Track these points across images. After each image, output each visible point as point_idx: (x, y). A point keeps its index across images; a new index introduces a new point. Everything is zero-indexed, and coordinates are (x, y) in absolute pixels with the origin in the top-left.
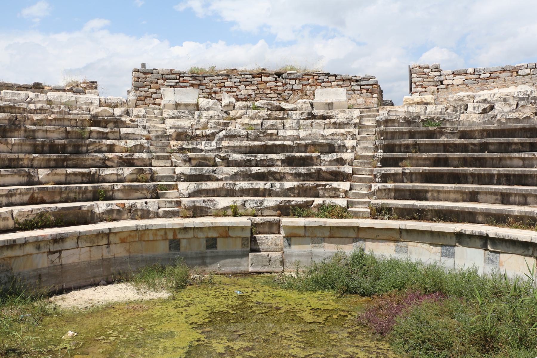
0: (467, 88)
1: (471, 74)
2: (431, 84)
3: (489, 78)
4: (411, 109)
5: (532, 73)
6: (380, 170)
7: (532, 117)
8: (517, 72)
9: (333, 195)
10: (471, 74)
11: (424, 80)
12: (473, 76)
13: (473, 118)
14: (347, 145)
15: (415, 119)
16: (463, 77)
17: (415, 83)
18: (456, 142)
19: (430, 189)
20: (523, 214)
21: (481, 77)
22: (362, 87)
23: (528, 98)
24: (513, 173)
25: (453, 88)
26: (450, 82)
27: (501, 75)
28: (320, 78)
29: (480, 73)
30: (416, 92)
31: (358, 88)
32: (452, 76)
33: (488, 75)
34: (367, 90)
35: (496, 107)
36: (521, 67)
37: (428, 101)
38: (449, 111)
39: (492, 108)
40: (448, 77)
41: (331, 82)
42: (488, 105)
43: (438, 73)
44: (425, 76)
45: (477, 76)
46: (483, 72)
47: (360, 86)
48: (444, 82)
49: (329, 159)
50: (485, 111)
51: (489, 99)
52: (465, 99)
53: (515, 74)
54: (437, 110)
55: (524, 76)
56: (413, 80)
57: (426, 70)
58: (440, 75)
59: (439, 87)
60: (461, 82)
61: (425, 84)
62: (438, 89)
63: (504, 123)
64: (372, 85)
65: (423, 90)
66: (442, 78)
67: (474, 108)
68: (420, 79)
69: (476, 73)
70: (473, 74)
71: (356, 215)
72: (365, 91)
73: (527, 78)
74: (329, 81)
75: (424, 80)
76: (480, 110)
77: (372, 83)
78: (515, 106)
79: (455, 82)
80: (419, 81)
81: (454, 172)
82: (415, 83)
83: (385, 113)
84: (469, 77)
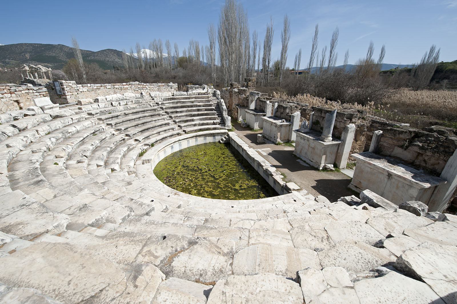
3: (97, 89)
12: (91, 88)
26: (82, 90)
28: (12, 88)
31: (38, 94)
34: (43, 95)
41: (21, 91)
43: (76, 86)
45: (92, 88)
48: (79, 90)
59: (78, 92)
60: (86, 90)
61: (71, 91)
65: (71, 94)
66: (78, 88)
68: (69, 89)
73: (110, 90)
74: (19, 91)
79: (84, 90)
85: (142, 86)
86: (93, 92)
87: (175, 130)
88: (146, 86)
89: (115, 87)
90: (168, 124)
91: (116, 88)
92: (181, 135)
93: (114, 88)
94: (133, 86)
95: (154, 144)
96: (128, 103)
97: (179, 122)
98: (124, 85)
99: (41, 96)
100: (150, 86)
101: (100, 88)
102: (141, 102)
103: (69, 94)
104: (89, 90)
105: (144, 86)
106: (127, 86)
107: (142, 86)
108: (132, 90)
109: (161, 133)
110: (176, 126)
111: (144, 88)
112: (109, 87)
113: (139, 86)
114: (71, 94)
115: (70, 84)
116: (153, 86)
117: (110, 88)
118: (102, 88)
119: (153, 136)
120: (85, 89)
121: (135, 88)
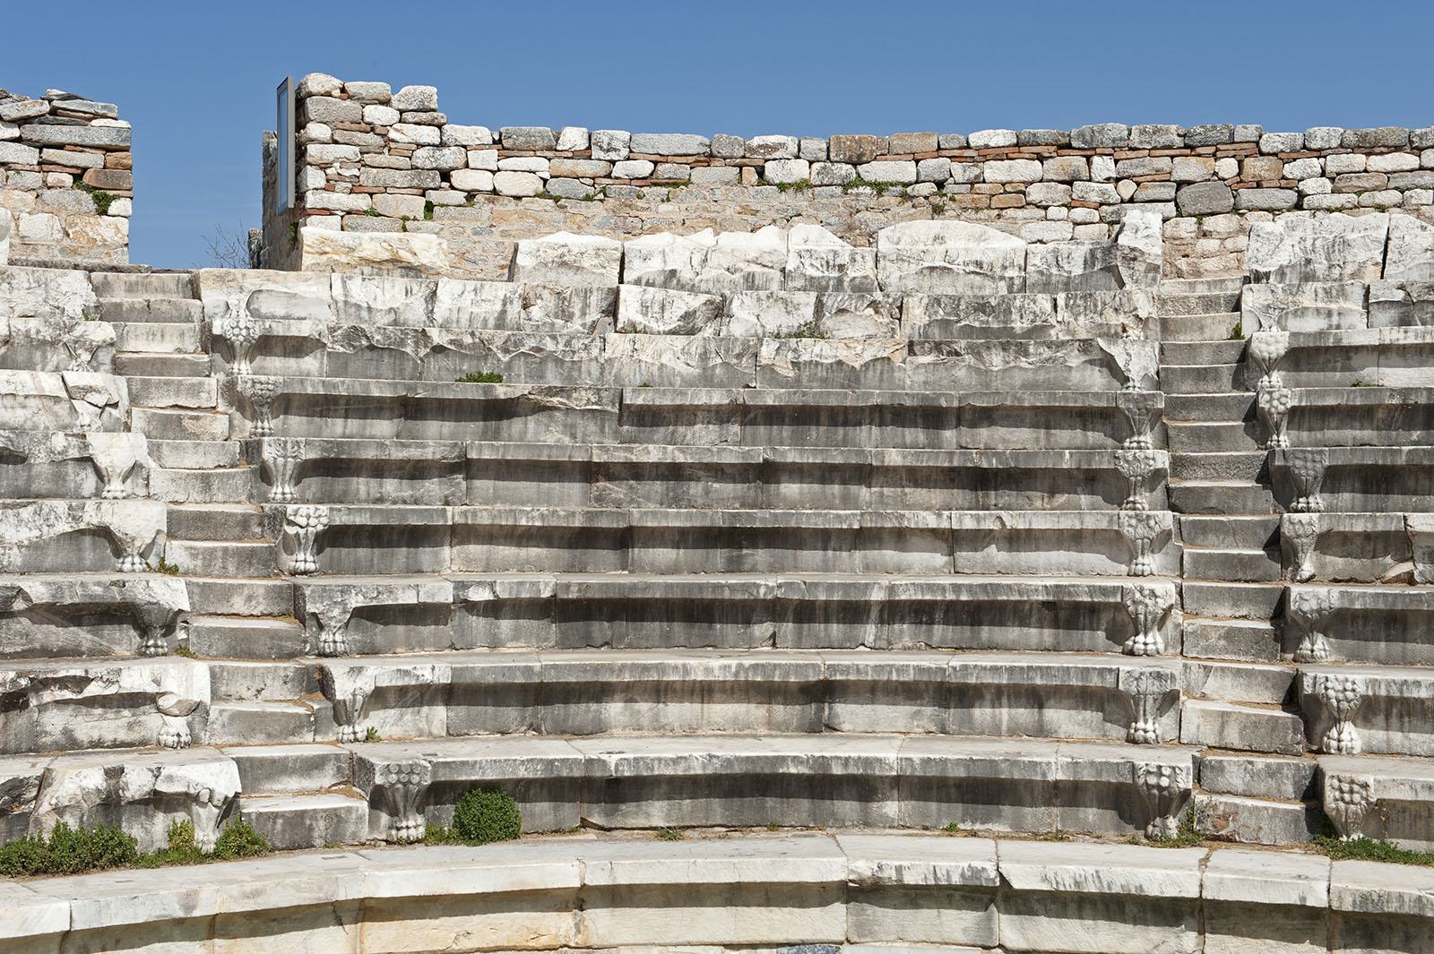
0: (559, 215)
1: (576, 155)
2: (400, 178)
3: (651, 180)
4: (360, 291)
5: (815, 180)
6: (345, 590)
7: (897, 359)
8: (761, 172)
9: (123, 736)
10: (576, 155)
11: (368, 159)
12: (584, 167)
13: (657, 357)
14: (102, 461)
15: (402, 342)
16: (541, 165)
17: (324, 167)
18: (644, 459)
19: (627, 678)
20: (1087, 776)
21: (618, 171)
22: (49, 154)
23: (840, 281)
24: (950, 597)
25: (497, 207)
26: (483, 182)
27: (699, 174)
29: (613, 156)
30: (329, 212)
31: (28, 155)
32: (494, 153)
33: (644, 168)
35: (735, 307)
36: (775, 148)
37: (424, 259)
38: (536, 312)
39: (720, 310)
40: (475, 158)
42: (703, 298)
43: (430, 134)
44: (371, 139)
45: (601, 168)
46: (625, 152)
47: (41, 146)
48: (456, 178)
49: (26, 535)
50: (688, 327)
51: (686, 275)
52: (586, 264)
53: (750, 175)
54: (485, 307)
55: (782, 187)
56: (312, 150)
57: (375, 114)
58: (442, 145)
59: (433, 196)
60: (531, 185)
61: (368, 178)
62: (429, 207)
63: (784, 383)
64: (107, 149)
65: (362, 202)
66: (449, 157)
67: (645, 308)
69: (596, 153)
70: (586, 154)
71: (297, 835)
72: (69, 180)
73: (801, 201)
75: (368, 159)
76: (672, 319)
77: (105, 141)
78: (808, 313)
79: (507, 183)
80: (344, 162)
81: (696, 595)
82: (324, 167)
83: (232, 301)
84: (568, 166)
85: (1228, 167)
86: (596, 209)
87: (1148, 726)
88: (1291, 170)
89: (876, 171)
90: (1111, 620)
91: (880, 188)
92: (1190, 837)
93: (860, 181)
94: (1104, 167)
95: (542, 811)
96: (828, 322)
97: (1339, 623)
98: (988, 154)
99: (52, 178)
100: (1359, 160)
101: (683, 172)
102: (1019, 325)
103: (341, 199)
104: (555, 187)
105: (1255, 166)
106: (1024, 169)
107: (1228, 167)
108: (1079, 214)
109: (847, 713)
110: (1229, 696)
111: (1247, 196)
112: (799, 170)
113: (1189, 168)
114: (362, 202)
115: (375, 114)
116: (1410, 161)
117: (801, 186)
118: (720, 172)
119: (675, 711)
120: (520, 175)
121: (1127, 189)
